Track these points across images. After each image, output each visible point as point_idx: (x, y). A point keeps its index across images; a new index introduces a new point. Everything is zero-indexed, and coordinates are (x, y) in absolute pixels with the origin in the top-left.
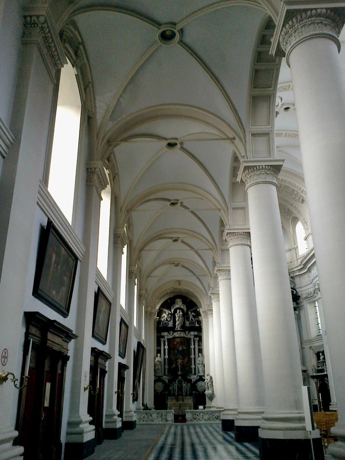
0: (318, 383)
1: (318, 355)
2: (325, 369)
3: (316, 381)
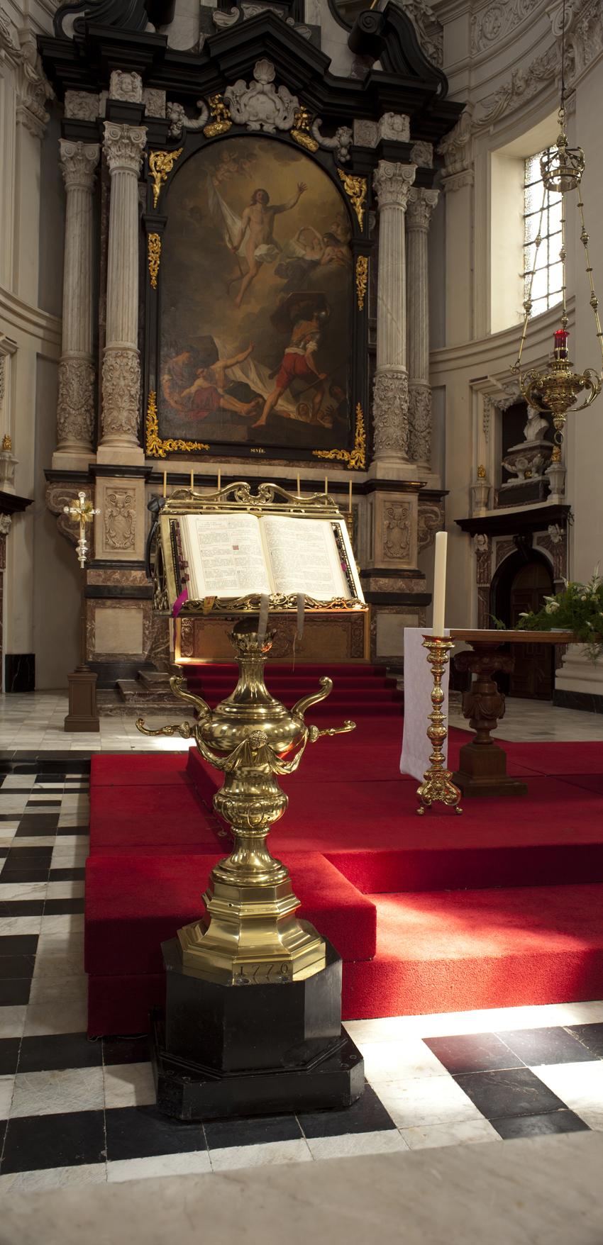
0: (494, 557)
1: (512, 420)
2: (554, 483)
3: (484, 548)
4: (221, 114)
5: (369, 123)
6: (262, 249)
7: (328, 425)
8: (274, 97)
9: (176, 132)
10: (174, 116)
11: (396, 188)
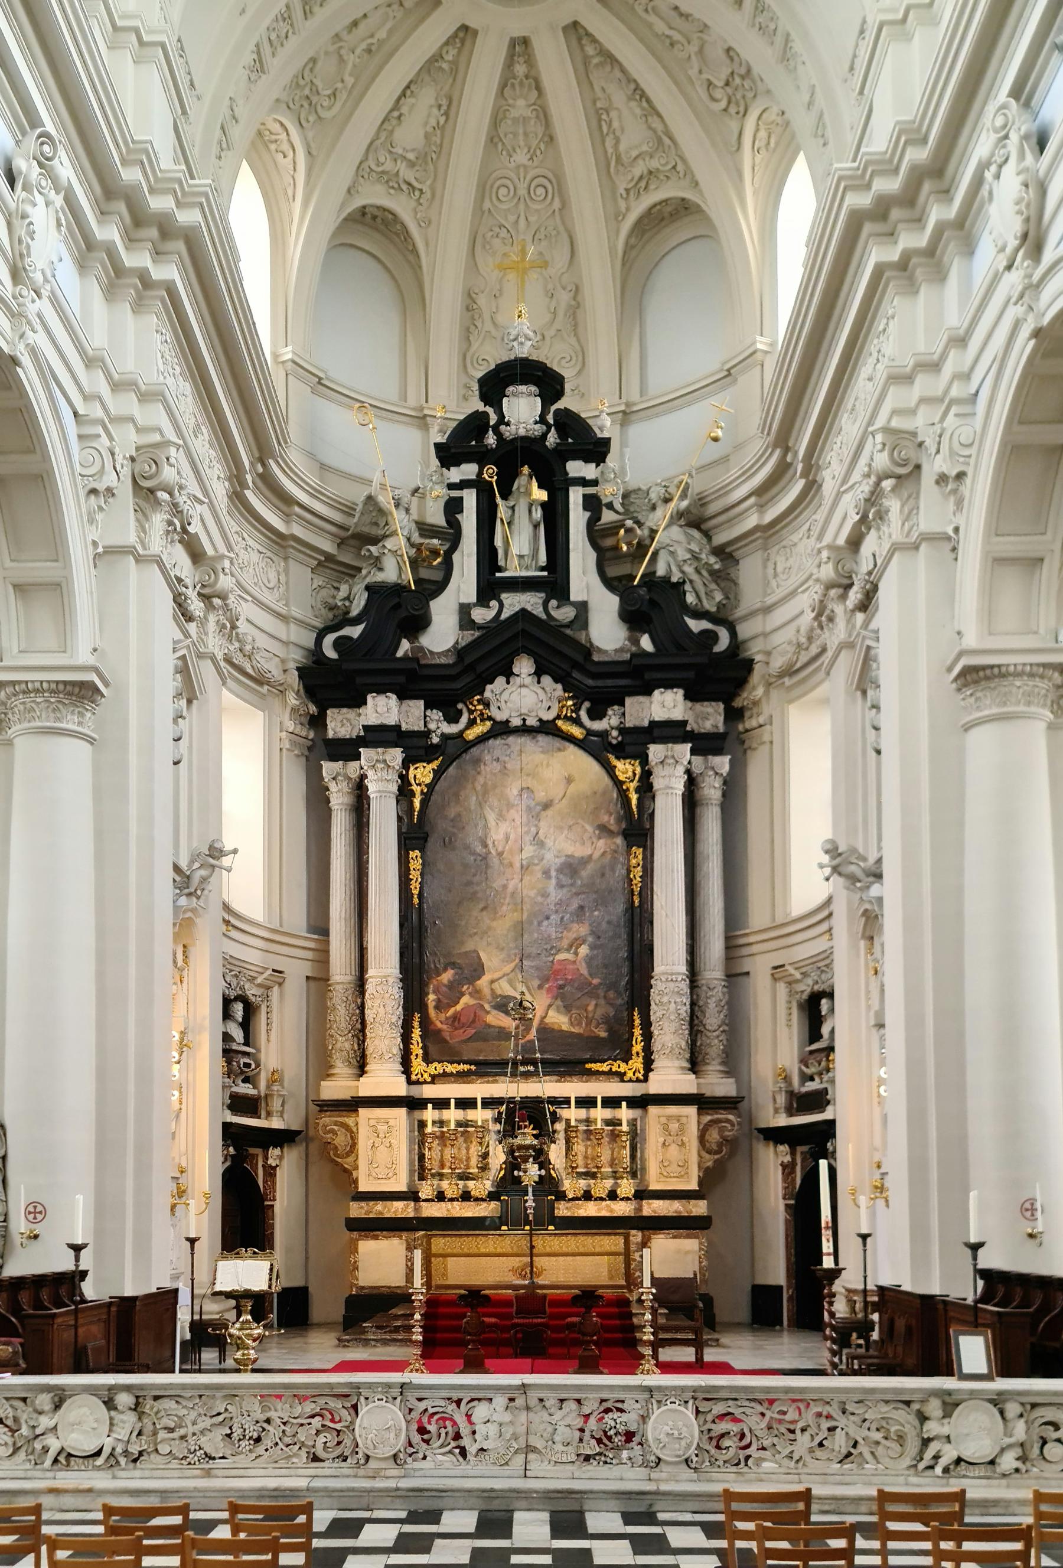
0: (798, 1169)
3: (788, 1159)
4: (482, 714)
5: (641, 699)
6: (529, 851)
7: (603, 1034)
8: (536, 688)
9: (435, 740)
10: (432, 726)
11: (671, 767)
